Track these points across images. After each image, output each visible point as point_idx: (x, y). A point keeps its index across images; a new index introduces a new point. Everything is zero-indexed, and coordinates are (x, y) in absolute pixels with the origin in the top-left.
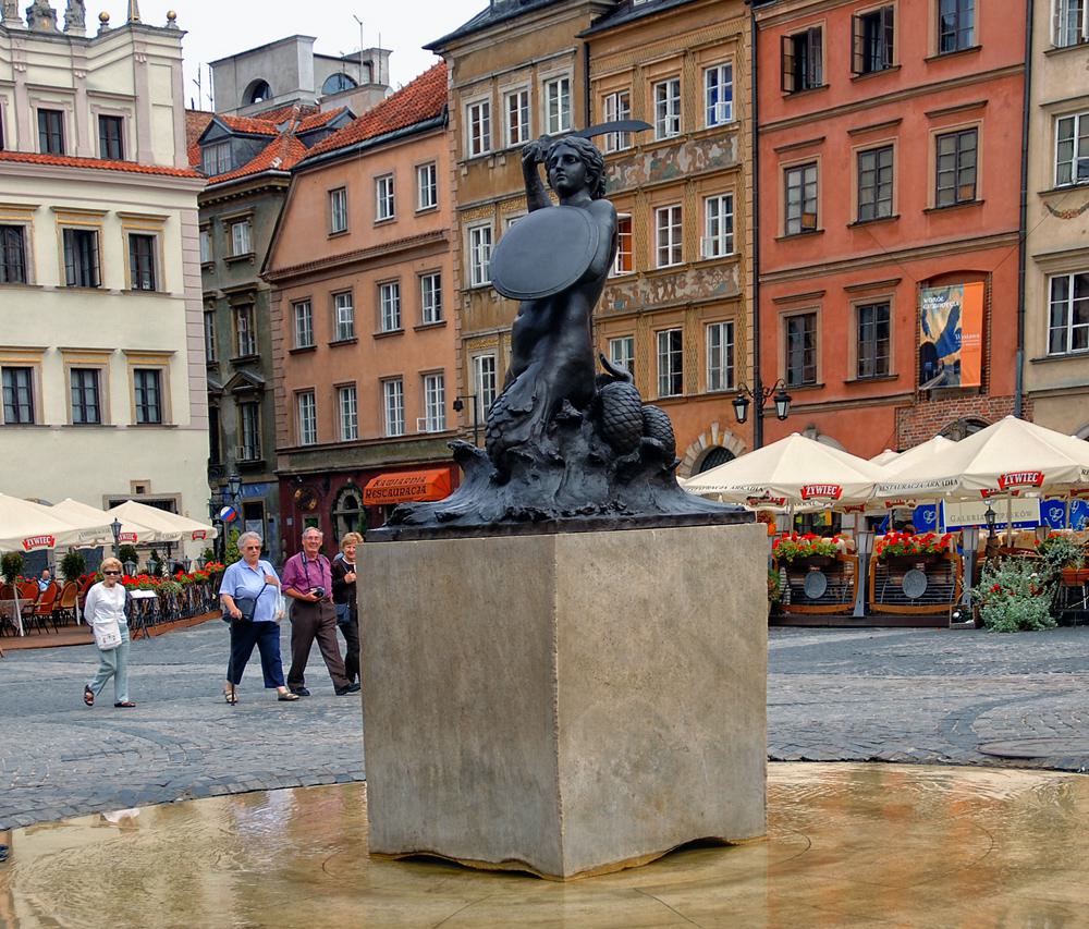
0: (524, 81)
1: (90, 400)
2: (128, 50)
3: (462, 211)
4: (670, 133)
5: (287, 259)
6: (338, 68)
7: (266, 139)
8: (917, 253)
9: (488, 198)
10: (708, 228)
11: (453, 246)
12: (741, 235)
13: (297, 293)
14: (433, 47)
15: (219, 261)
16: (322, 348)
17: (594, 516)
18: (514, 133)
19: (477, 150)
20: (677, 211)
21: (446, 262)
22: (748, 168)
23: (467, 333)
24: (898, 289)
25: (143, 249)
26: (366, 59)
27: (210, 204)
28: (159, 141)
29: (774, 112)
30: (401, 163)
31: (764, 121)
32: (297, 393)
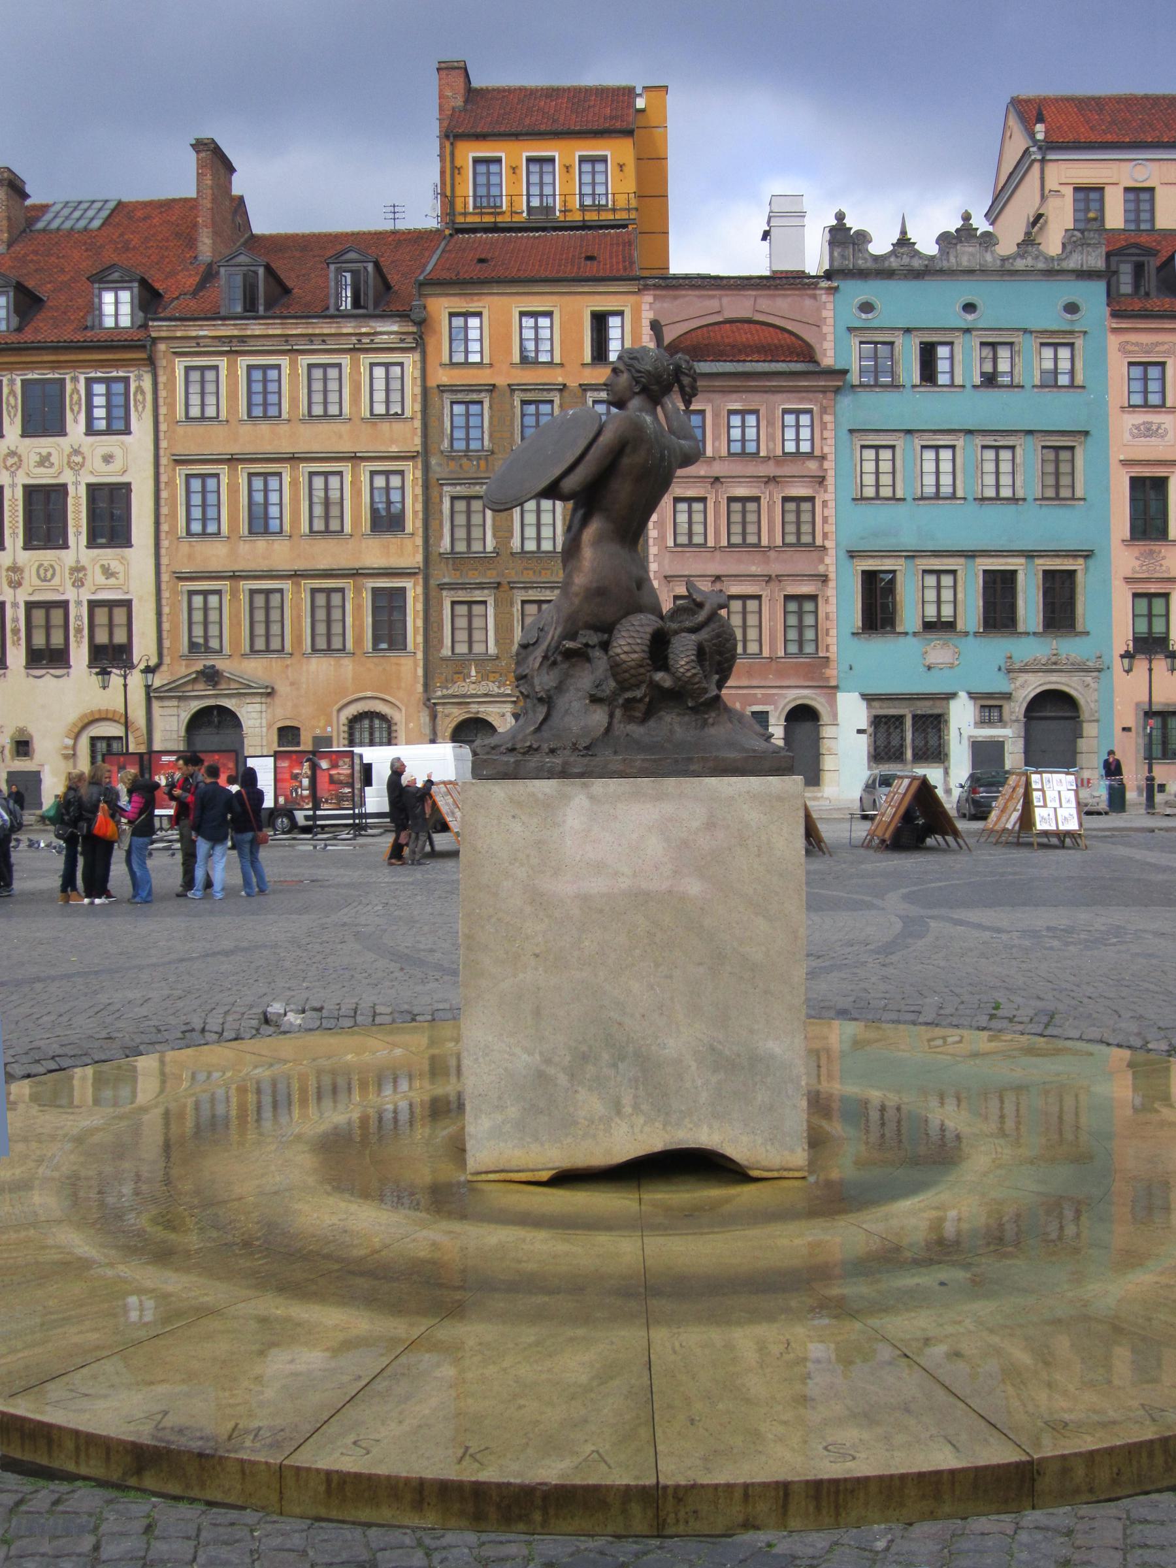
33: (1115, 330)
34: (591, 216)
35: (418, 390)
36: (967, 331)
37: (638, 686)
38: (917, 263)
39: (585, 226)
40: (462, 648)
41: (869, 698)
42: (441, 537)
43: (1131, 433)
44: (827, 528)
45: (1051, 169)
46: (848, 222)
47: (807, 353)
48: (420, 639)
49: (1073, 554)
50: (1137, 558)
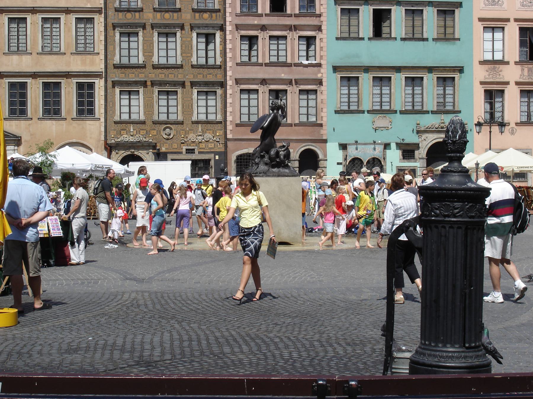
41: (344, 147)
42: (114, 55)
43: (484, 4)
44: (322, 53)
48: (103, 111)
50: (487, 71)
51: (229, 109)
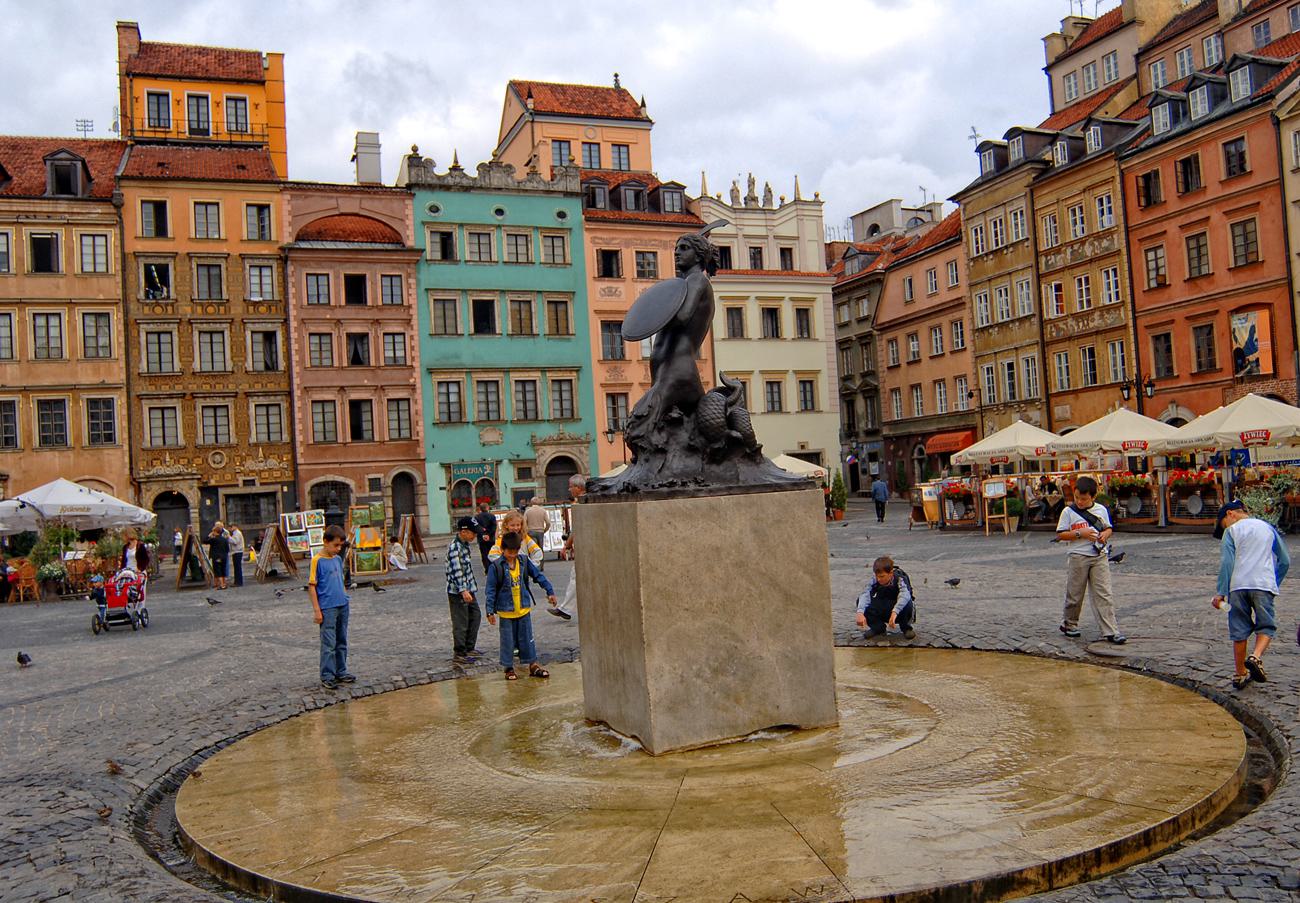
0: (1000, 212)
1: (776, 398)
2: (795, 214)
3: (971, 286)
4: (1080, 235)
5: (885, 317)
6: (914, 214)
7: (878, 254)
8: (1226, 294)
9: (985, 278)
10: (1105, 287)
11: (968, 305)
12: (1123, 289)
13: (890, 335)
14: (953, 199)
15: (853, 320)
16: (904, 365)
17: (677, 488)
18: (997, 241)
19: (978, 252)
20: (1087, 279)
21: (964, 314)
22: (1124, 251)
23: (978, 354)
24: (1217, 316)
25: (803, 315)
26: (929, 209)
27: (837, 293)
28: (810, 259)
29: (1137, 218)
30: (939, 262)
31: (1131, 224)
32: (892, 390)
33: (587, 229)
34: (236, 138)
35: (119, 255)
36: (499, 227)
37: (719, 440)
38: (465, 182)
39: (231, 145)
40: (158, 442)
41: (447, 467)
42: (140, 361)
44: (414, 354)
45: (537, 127)
46: (421, 153)
47: (396, 239)
48: (126, 436)
49: (570, 369)
51: (298, 427)
